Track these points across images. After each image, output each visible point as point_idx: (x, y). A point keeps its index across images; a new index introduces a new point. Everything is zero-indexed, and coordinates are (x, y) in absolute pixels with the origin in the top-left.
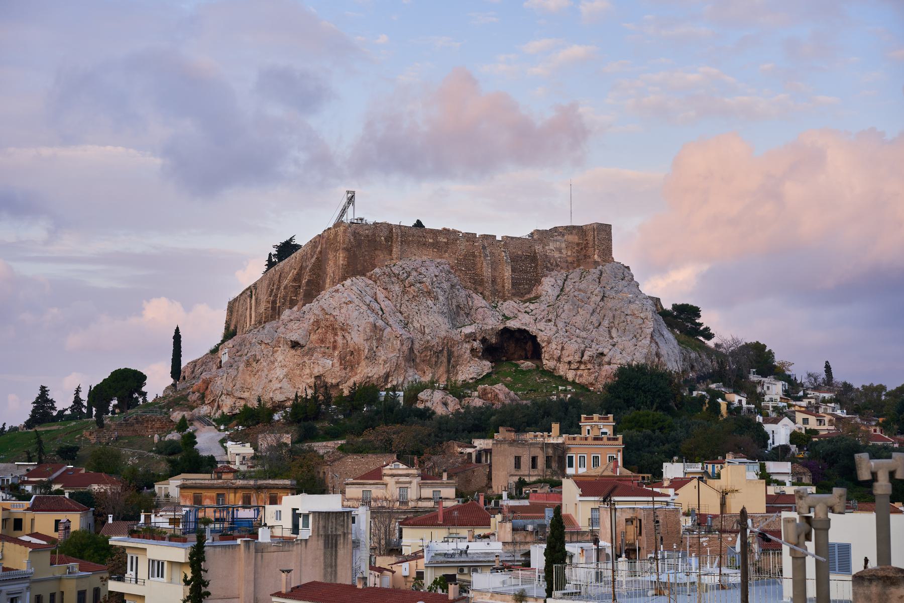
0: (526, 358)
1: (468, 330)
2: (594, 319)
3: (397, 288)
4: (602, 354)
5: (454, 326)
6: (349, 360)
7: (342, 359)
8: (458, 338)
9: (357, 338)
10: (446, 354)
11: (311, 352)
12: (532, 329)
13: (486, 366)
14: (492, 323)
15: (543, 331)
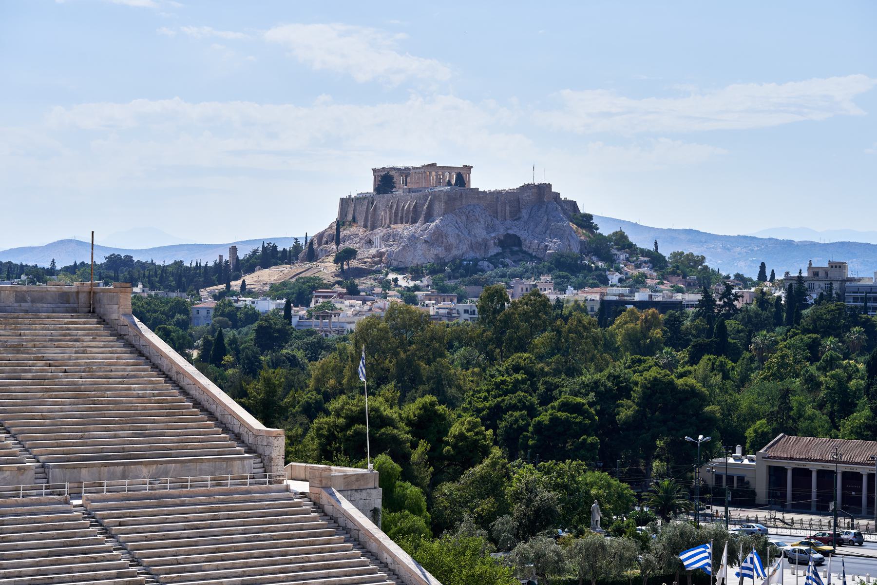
0: (515, 245)
1: (493, 235)
2: (544, 230)
3: (464, 217)
4: (547, 246)
5: (488, 233)
6: (448, 249)
7: (446, 248)
8: (488, 238)
9: (452, 240)
10: (485, 245)
11: (432, 245)
12: (519, 235)
13: (500, 250)
14: (502, 232)
15: (522, 235)
